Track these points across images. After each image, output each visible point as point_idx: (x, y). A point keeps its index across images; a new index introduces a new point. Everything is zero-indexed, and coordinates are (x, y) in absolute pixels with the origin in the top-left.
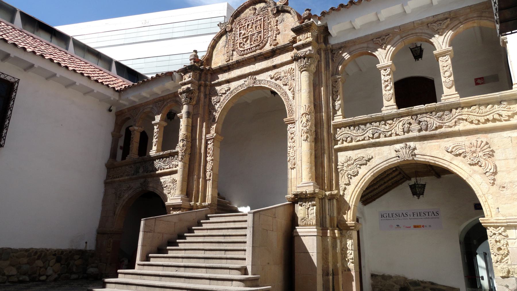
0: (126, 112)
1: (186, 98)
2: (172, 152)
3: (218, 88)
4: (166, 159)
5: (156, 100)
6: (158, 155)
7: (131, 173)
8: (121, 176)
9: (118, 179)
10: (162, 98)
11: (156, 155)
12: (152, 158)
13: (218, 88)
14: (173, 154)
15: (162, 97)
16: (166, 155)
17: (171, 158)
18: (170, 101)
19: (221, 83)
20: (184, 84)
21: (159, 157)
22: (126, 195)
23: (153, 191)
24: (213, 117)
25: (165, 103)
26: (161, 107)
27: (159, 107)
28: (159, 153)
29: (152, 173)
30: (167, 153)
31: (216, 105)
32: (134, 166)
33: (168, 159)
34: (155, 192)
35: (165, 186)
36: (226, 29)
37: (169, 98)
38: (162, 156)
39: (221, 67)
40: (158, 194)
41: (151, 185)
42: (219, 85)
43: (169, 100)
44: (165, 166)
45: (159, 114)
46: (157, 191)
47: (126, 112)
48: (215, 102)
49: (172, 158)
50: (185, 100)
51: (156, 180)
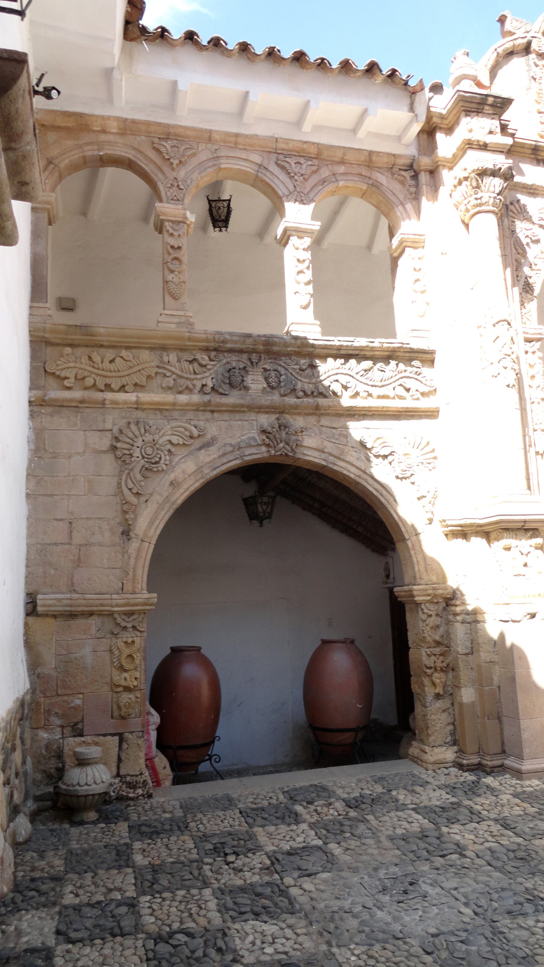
0: (104, 131)
1: (498, 194)
2: (406, 348)
3: (524, 199)
4: (374, 364)
5: (283, 146)
6: (347, 346)
7: (199, 384)
8: (136, 385)
9: (132, 397)
10: (313, 150)
11: (338, 343)
12: (311, 350)
13: (524, 199)
14: (407, 355)
15: (313, 143)
16: (378, 353)
17: (397, 365)
18: (345, 174)
19: (536, 192)
20: (479, 145)
21: (343, 352)
22: (190, 466)
23: (324, 463)
24: (523, 280)
25: (325, 172)
26: (305, 180)
27: (302, 175)
28: (352, 339)
29: (321, 401)
30: (385, 345)
31: (530, 248)
32: (211, 360)
33: (379, 365)
34: (335, 468)
35: (386, 452)
36: (529, 44)
37: (342, 162)
38: (357, 352)
39: (540, 146)
40: (352, 476)
41: (309, 441)
42: (530, 193)
43: (342, 169)
44: (372, 386)
45: (308, 203)
46: (343, 464)
47: (104, 131)
48: (527, 236)
49: (402, 366)
50: (495, 198)
51: (334, 428)
